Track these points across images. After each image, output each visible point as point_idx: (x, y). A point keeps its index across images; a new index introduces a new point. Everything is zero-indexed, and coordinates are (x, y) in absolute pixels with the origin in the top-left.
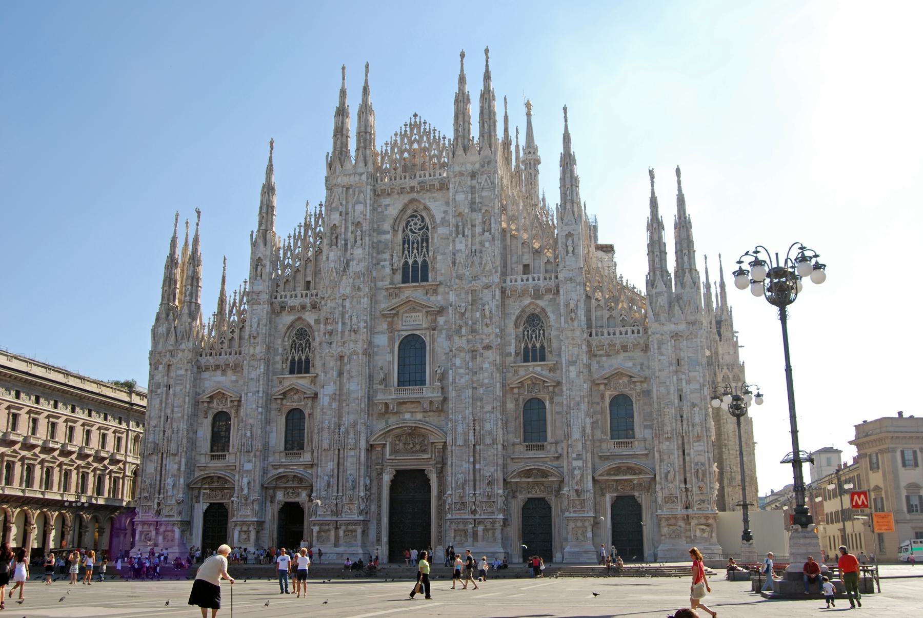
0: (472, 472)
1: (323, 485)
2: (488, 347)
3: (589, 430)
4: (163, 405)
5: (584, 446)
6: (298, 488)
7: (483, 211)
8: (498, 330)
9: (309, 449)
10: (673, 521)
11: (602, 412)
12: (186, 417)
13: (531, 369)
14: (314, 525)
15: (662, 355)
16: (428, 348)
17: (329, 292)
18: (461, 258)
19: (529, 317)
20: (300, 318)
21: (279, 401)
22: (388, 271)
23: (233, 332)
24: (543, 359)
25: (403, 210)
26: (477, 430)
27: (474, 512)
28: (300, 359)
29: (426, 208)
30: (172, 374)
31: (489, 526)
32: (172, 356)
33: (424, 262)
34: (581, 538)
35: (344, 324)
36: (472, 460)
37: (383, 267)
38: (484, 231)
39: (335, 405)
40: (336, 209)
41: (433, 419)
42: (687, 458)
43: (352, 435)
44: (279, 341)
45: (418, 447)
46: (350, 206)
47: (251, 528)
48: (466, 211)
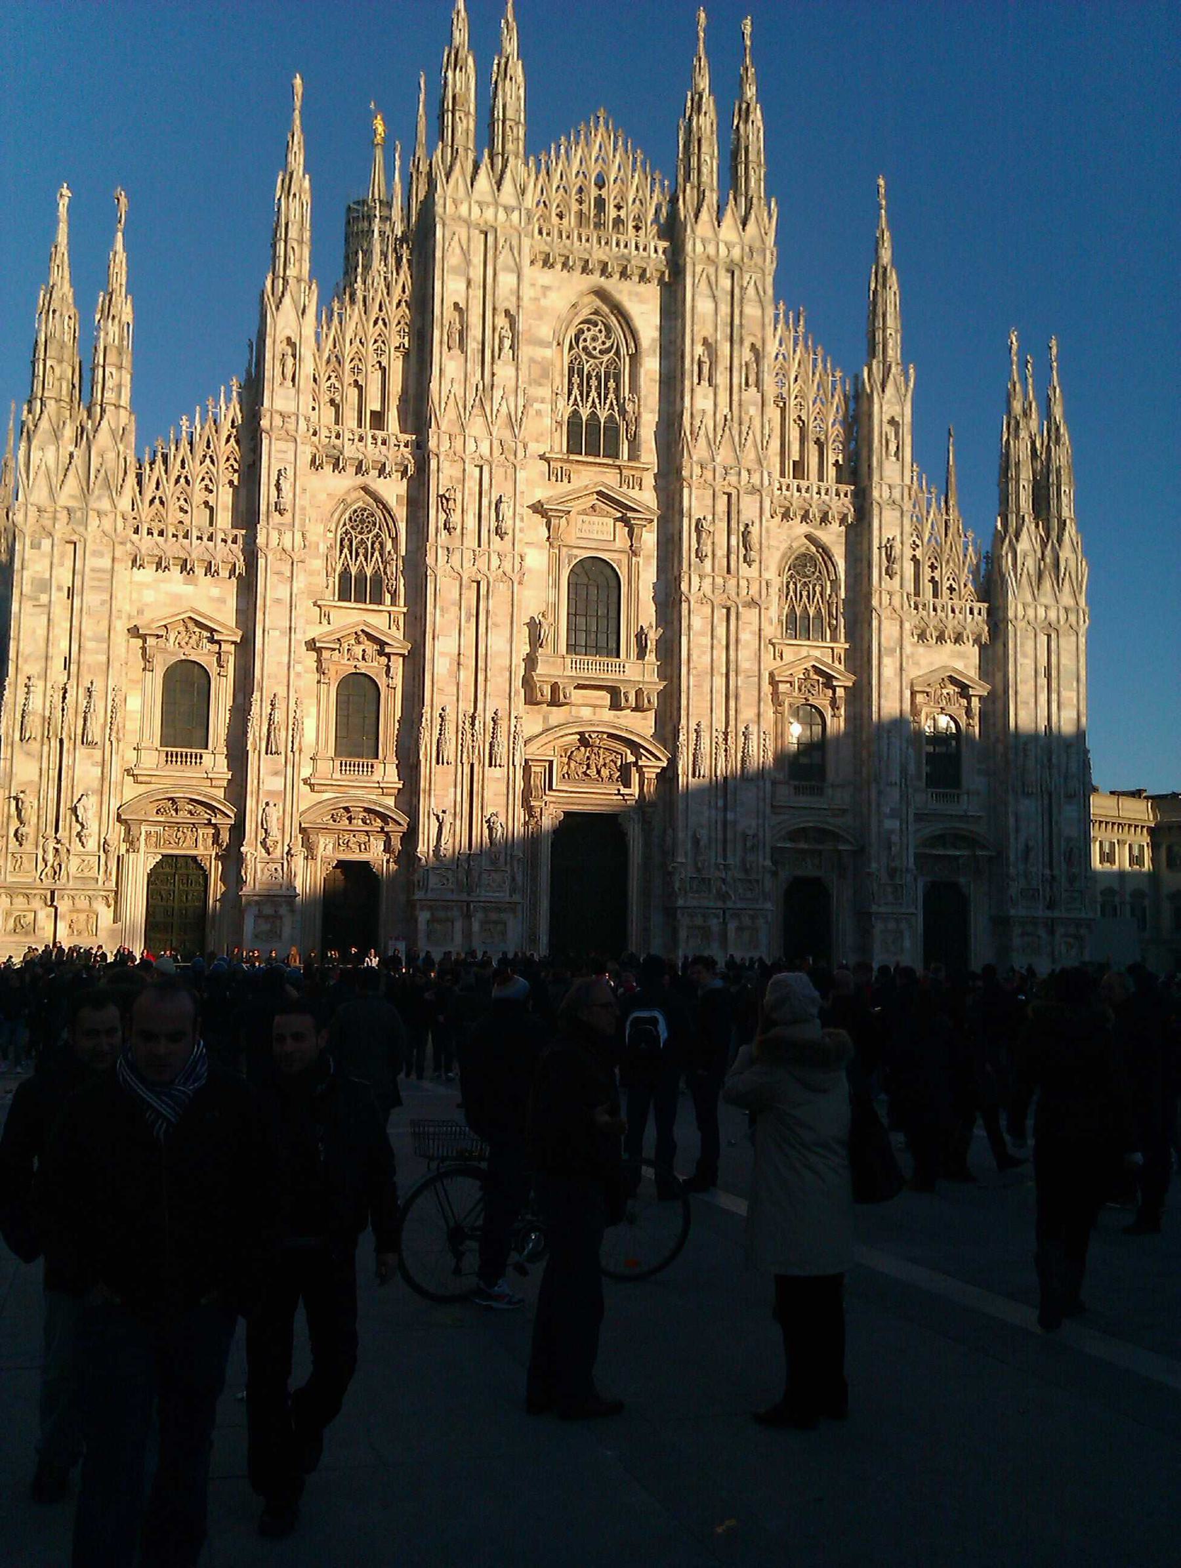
0: (719, 827)
2: (753, 603)
3: (912, 769)
7: (747, 344)
14: (422, 909)
15: (1025, 656)
19: (796, 559)
27: (723, 897)
28: (361, 570)
36: (720, 803)
37: (539, 413)
38: (747, 384)
44: (321, 528)
45: (605, 772)
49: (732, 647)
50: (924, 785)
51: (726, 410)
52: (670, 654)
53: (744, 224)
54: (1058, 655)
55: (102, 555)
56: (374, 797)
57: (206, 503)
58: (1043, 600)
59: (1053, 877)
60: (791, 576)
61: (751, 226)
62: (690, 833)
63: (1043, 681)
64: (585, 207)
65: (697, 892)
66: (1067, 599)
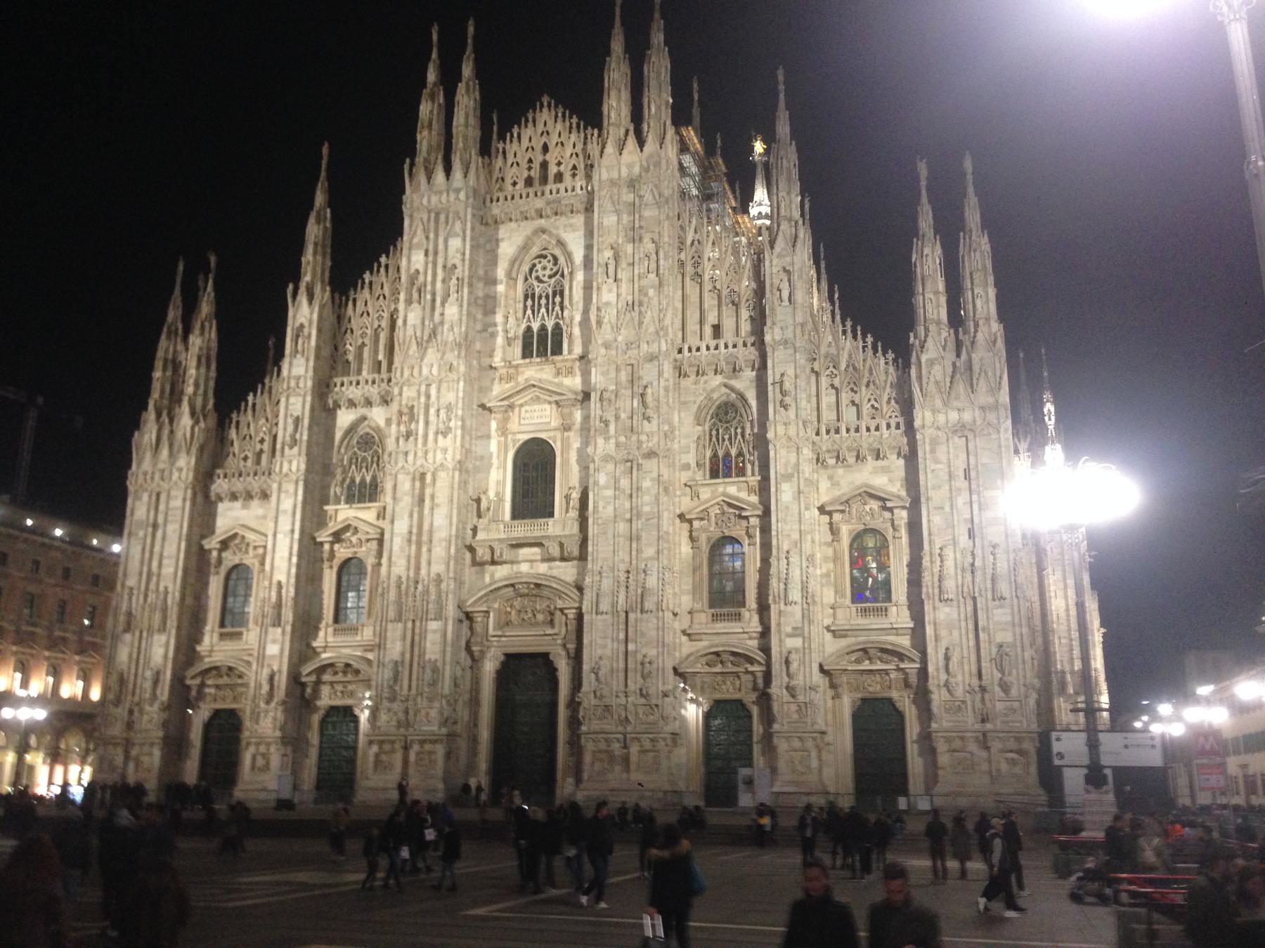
0: (621, 657)
1: (386, 677)
2: (651, 454)
4: (147, 555)
5: (807, 617)
8: (666, 428)
9: (372, 621)
10: (958, 744)
11: (836, 558)
12: (180, 573)
13: (721, 489)
14: (371, 743)
15: (937, 461)
16: (558, 460)
17: (406, 374)
18: (610, 316)
19: (719, 407)
20: (364, 418)
22: (500, 340)
24: (741, 472)
25: (525, 248)
26: (632, 588)
28: (363, 480)
29: (561, 243)
30: (162, 507)
31: (648, 745)
33: (557, 328)
34: (800, 768)
36: (622, 636)
40: (419, 246)
41: (567, 572)
42: (982, 635)
45: (540, 617)
49: (634, 495)
50: (848, 601)
51: (630, 298)
53: (641, 143)
54: (976, 456)
55: (176, 497)
56: (359, 654)
57: (262, 451)
58: (956, 404)
59: (983, 689)
60: (714, 424)
61: (651, 145)
63: (961, 483)
64: (532, 173)
65: (600, 719)
66: (983, 397)
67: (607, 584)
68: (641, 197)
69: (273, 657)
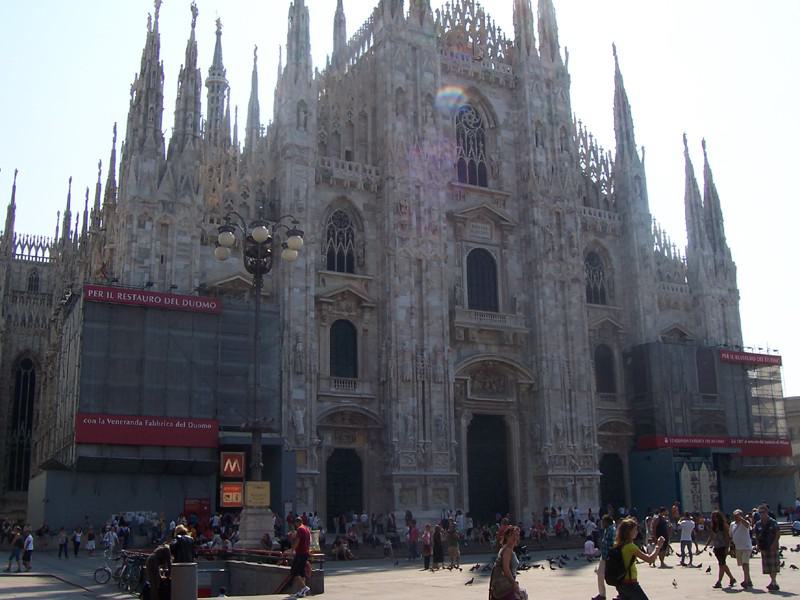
0: (568, 421)
2: (576, 280)
6: (355, 430)
7: (560, 127)
15: (713, 317)
21: (324, 306)
23: (245, 195)
24: (604, 303)
27: (573, 468)
28: (341, 253)
32: (172, 212)
33: (482, 164)
35: (419, 218)
36: (568, 407)
39: (414, 322)
40: (402, 69)
43: (440, 364)
45: (494, 387)
46: (418, 71)
47: (308, 484)
48: (545, 120)
49: (567, 306)
52: (529, 310)
55: (185, 234)
57: (245, 203)
62: (553, 427)
63: (722, 331)
67: (557, 370)
68: (556, 94)
69: (302, 403)
